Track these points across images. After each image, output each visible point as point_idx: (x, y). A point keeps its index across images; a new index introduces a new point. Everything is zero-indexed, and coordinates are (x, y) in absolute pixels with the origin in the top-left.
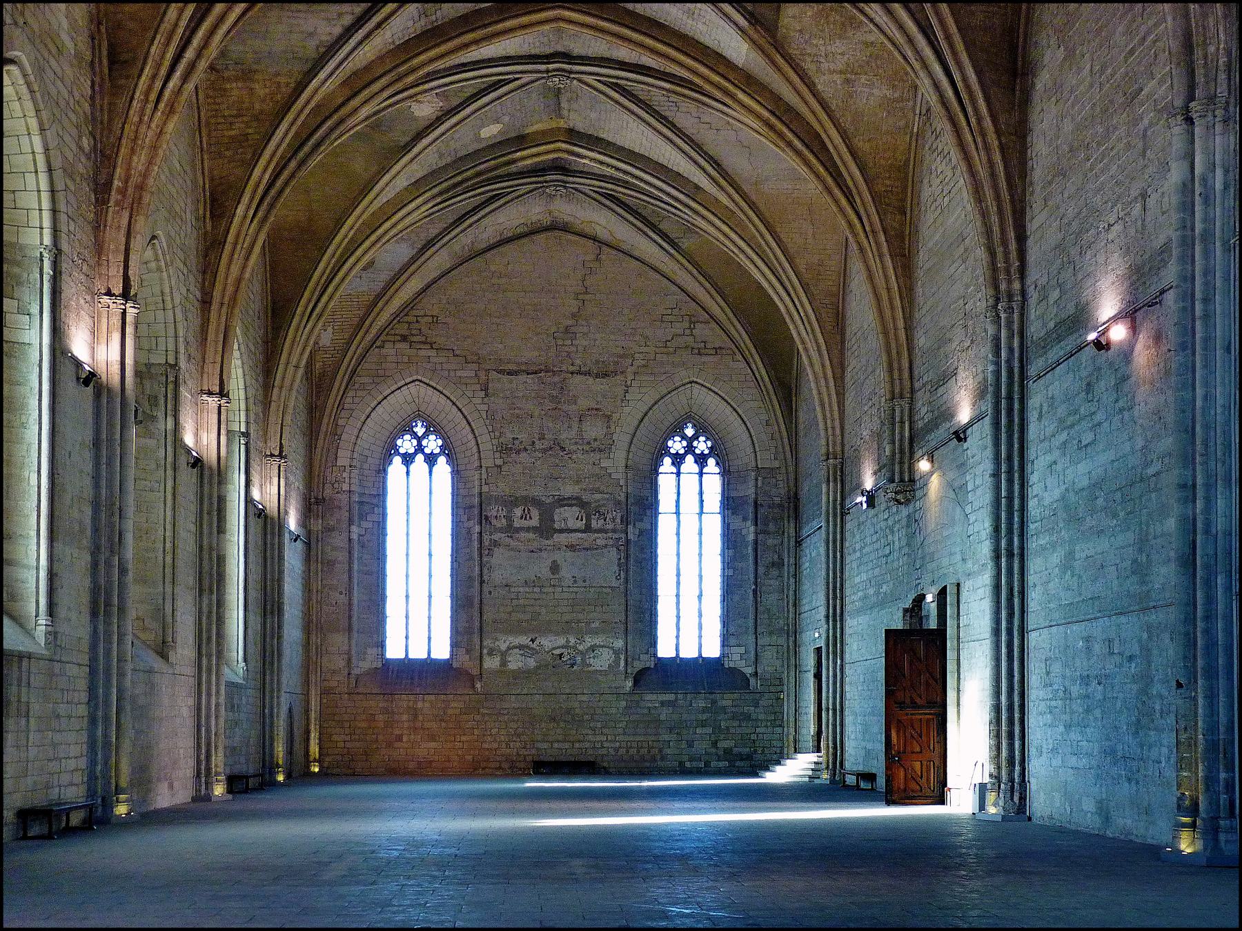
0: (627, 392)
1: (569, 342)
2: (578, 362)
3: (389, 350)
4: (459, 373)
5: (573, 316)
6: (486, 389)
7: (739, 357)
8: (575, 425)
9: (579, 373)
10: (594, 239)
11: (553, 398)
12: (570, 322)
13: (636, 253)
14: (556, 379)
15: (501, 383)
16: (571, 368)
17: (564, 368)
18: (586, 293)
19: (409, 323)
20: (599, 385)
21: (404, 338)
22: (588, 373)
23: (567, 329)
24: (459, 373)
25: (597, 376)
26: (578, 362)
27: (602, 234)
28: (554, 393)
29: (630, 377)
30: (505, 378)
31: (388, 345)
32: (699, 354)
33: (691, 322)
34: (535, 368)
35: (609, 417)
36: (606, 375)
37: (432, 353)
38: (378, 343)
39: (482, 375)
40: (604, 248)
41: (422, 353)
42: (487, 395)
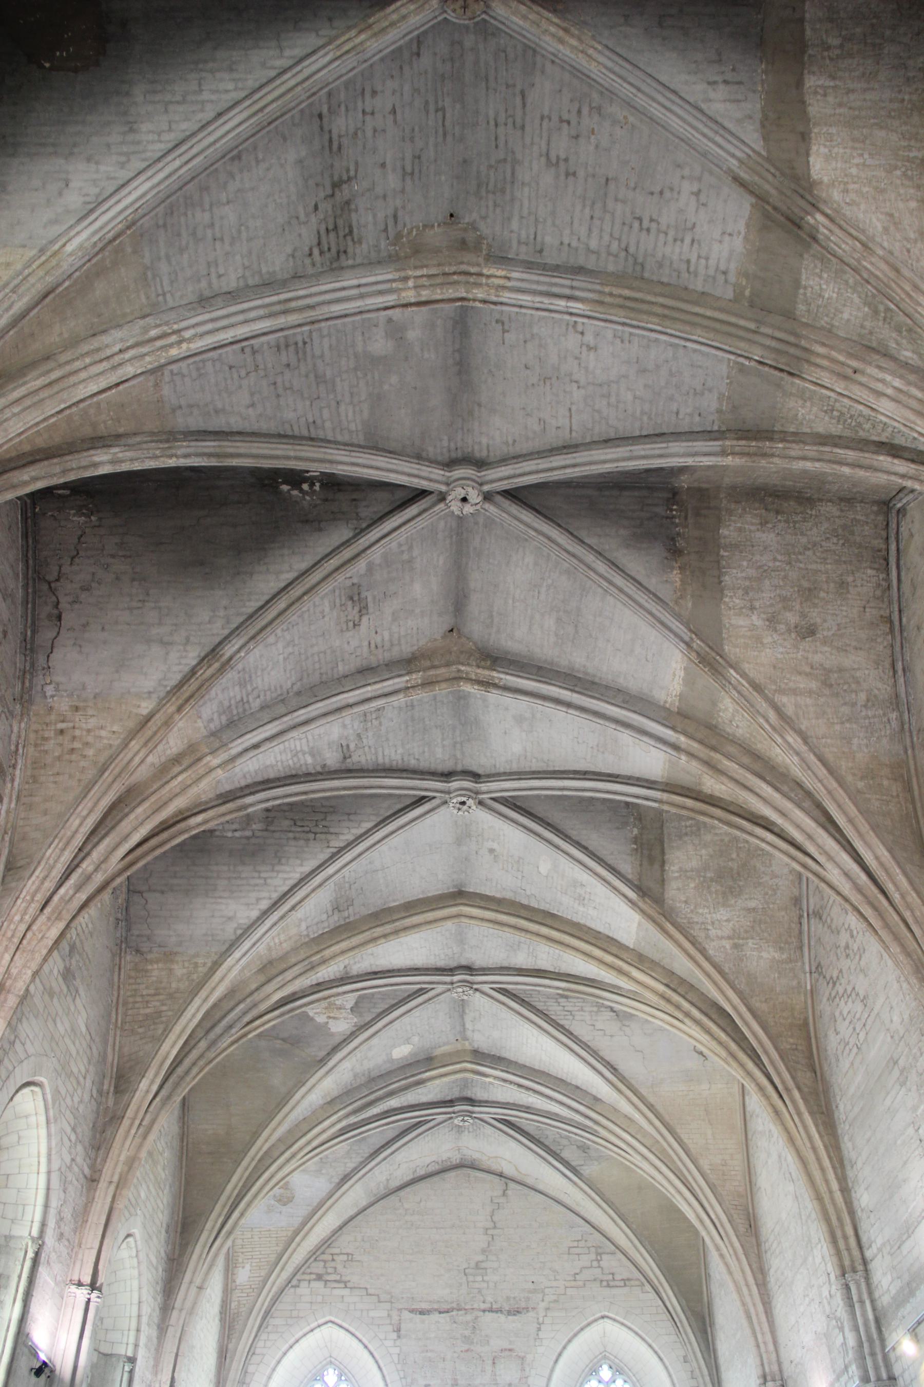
0: (539, 1329)
1: (479, 1278)
2: (489, 1299)
3: (304, 1289)
4: (372, 1314)
5: (483, 1251)
6: (399, 1330)
7: (648, 1287)
8: (489, 1368)
9: (491, 1310)
10: (501, 1175)
11: (467, 1339)
12: (481, 1258)
13: (540, 1187)
14: (469, 1317)
15: (413, 1323)
16: (483, 1306)
17: (476, 1306)
18: (495, 1227)
19: (325, 1262)
20: (511, 1323)
21: (319, 1277)
22: (499, 1311)
23: (477, 1266)
24: (372, 1314)
25: (509, 1313)
26: (489, 1299)
27: (508, 1170)
28: (467, 1333)
29: (542, 1313)
30: (418, 1317)
31: (304, 1284)
32: (608, 1286)
33: (597, 1254)
34: (445, 1306)
35: (523, 1358)
36: (517, 1312)
37: (346, 1292)
38: (294, 1282)
39: (394, 1314)
40: (512, 1185)
41: (337, 1292)
42: (399, 1337)
